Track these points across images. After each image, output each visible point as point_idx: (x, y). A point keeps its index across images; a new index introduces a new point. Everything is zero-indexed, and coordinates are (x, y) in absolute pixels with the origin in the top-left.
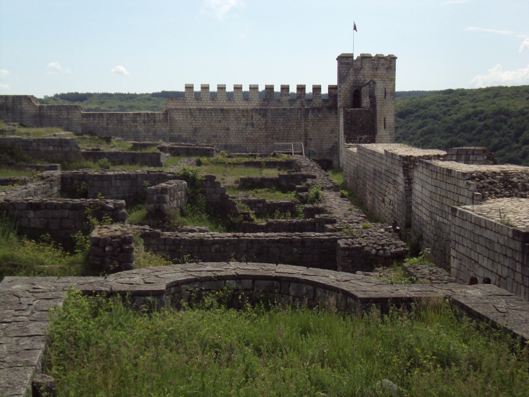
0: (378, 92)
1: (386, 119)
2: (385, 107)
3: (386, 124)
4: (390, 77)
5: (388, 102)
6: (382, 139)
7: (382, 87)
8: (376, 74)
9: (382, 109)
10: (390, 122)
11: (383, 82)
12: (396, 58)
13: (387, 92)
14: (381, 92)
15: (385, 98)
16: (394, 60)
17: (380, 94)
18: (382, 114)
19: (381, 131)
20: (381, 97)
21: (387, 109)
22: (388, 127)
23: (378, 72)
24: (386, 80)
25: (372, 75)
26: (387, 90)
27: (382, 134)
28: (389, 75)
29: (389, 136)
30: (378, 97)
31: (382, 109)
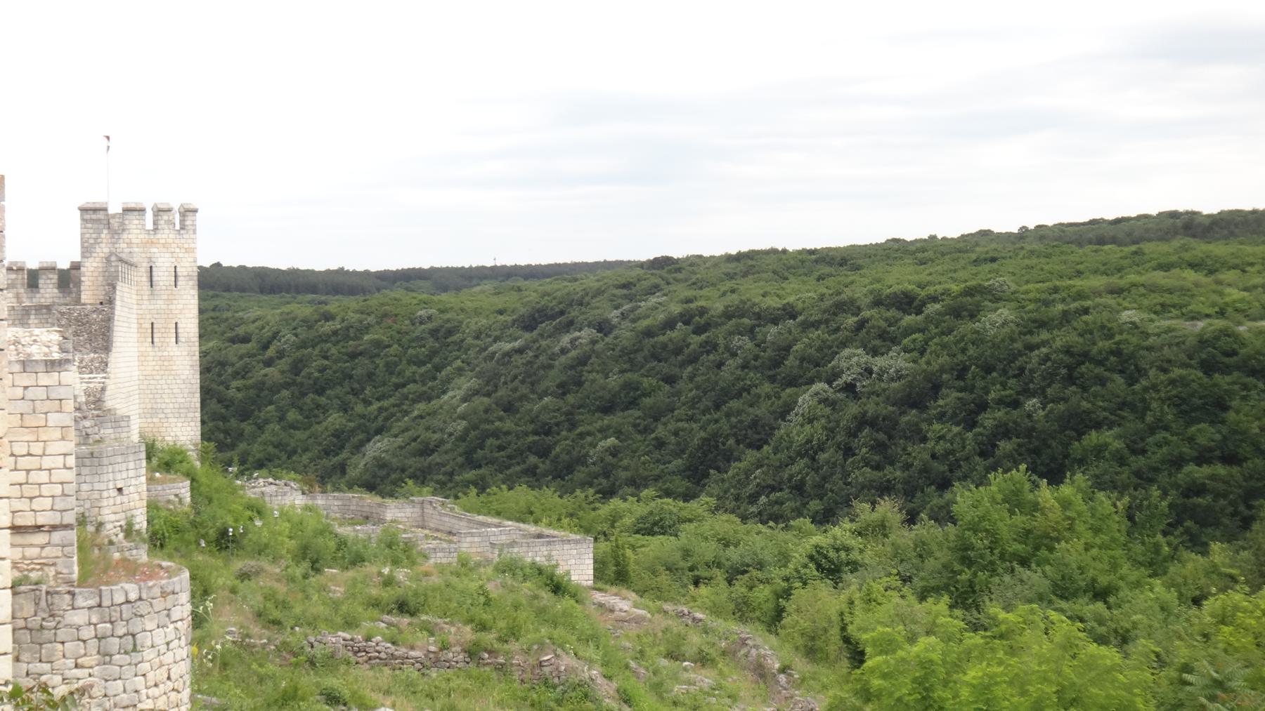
0: (160, 274)
1: (179, 325)
2: (175, 302)
3: (180, 335)
4: (186, 246)
5: (182, 292)
6: (171, 363)
7: (166, 264)
8: (155, 241)
9: (170, 307)
10: (188, 330)
11: (170, 255)
12: (195, 211)
13: (179, 274)
14: (166, 274)
15: (176, 286)
16: (191, 214)
17: (164, 278)
18: (170, 316)
19: (169, 349)
20: (167, 283)
21: (181, 307)
22: (183, 340)
23: (159, 236)
24: (178, 250)
25: (148, 242)
26: (178, 269)
27: (172, 354)
28: (182, 241)
29: (187, 358)
30: (161, 283)
31: (170, 307)
